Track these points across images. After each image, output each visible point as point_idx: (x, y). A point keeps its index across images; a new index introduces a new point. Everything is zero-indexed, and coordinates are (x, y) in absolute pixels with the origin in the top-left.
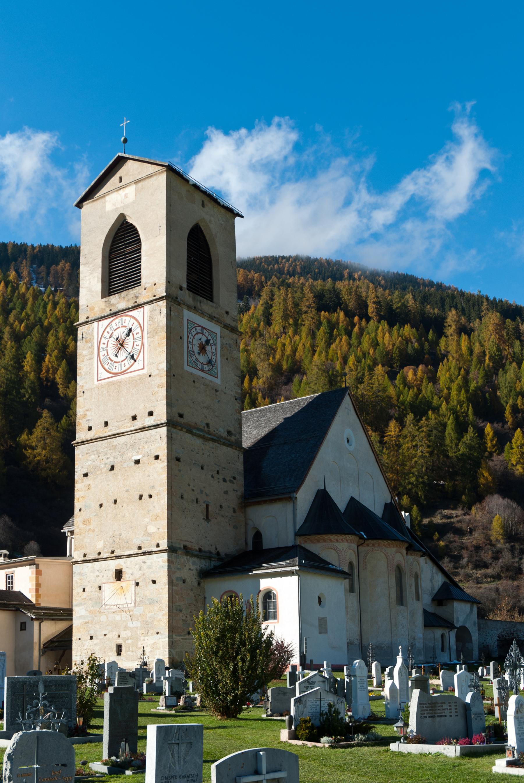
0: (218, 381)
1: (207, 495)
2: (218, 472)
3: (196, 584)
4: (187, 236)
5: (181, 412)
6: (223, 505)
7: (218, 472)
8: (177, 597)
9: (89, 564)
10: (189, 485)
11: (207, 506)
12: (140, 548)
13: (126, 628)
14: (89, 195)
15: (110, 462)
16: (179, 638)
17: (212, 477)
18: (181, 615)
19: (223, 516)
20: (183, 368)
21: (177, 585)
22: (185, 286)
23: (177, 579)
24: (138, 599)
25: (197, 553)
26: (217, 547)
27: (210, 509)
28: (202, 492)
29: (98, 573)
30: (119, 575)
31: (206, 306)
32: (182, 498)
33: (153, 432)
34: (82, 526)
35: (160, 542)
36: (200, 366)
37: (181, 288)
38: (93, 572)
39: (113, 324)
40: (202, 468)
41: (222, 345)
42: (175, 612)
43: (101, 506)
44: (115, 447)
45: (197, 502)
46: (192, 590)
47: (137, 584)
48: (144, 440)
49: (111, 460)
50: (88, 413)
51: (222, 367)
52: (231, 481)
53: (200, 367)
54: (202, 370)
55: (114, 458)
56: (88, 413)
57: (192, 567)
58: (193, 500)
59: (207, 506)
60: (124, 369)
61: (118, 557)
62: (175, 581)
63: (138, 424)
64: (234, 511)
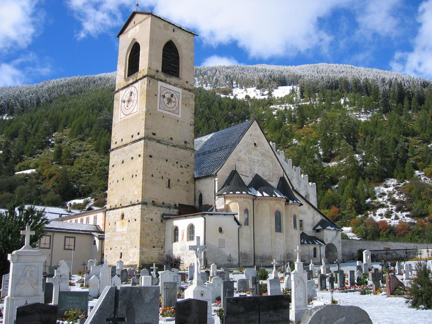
0: (180, 116)
1: (169, 174)
2: (177, 163)
3: (160, 221)
4: (163, 46)
5: (154, 132)
6: (180, 180)
7: (177, 163)
9: (112, 211)
10: (157, 169)
11: (169, 180)
13: (124, 244)
14: (122, 32)
15: (122, 159)
16: (147, 249)
17: (173, 165)
18: (149, 237)
19: (179, 185)
21: (147, 222)
22: (160, 70)
23: (147, 218)
24: (129, 229)
25: (162, 205)
26: (175, 201)
27: (171, 182)
28: (166, 173)
29: (114, 216)
30: (123, 216)
31: (174, 80)
32: (152, 176)
33: (139, 143)
34: (110, 192)
35: (139, 199)
37: (157, 71)
38: (113, 215)
39: (127, 91)
40: (167, 161)
42: (145, 235)
43: (118, 181)
44: (124, 151)
45: (162, 178)
46: (157, 224)
47: (129, 221)
48: (135, 147)
49: (123, 158)
50: (116, 135)
52: (185, 167)
53: (168, 109)
55: (124, 157)
56: (116, 135)
58: (160, 177)
59: (169, 180)
60: (130, 112)
61: (122, 207)
62: (145, 219)
63: (134, 139)
64: (187, 182)
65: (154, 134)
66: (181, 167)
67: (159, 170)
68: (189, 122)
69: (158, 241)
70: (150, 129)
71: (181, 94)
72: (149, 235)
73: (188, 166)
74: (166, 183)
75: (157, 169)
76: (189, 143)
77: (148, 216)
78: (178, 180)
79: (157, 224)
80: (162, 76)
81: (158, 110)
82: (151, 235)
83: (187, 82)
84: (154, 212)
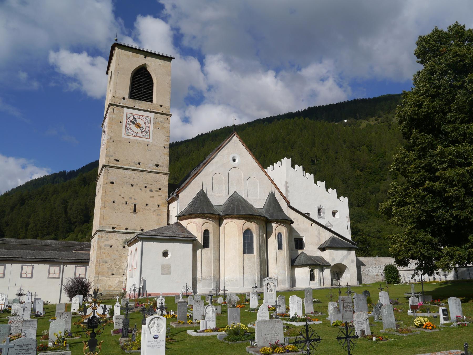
0: (150, 140)
1: (135, 199)
2: (146, 187)
6: (149, 204)
7: (146, 187)
8: (104, 255)
11: (135, 205)
12: (127, 229)
16: (104, 277)
18: (106, 265)
19: (148, 210)
20: (121, 137)
21: (104, 249)
22: (127, 96)
23: (105, 245)
25: (124, 231)
27: (137, 207)
31: (144, 105)
32: (114, 202)
37: (124, 98)
41: (154, 123)
45: (126, 204)
51: (153, 133)
52: (156, 191)
53: (136, 135)
57: (118, 239)
59: (135, 205)
62: (103, 247)
65: (117, 161)
66: (151, 191)
67: (122, 196)
68: (163, 145)
69: (119, 268)
70: (112, 156)
71: (152, 119)
72: (107, 263)
73: (160, 189)
74: (130, 209)
75: (120, 195)
76: (162, 167)
77: (106, 243)
78: (147, 205)
79: (117, 251)
80: (131, 103)
81: (123, 136)
82: (109, 263)
83: (161, 106)
84: (114, 238)
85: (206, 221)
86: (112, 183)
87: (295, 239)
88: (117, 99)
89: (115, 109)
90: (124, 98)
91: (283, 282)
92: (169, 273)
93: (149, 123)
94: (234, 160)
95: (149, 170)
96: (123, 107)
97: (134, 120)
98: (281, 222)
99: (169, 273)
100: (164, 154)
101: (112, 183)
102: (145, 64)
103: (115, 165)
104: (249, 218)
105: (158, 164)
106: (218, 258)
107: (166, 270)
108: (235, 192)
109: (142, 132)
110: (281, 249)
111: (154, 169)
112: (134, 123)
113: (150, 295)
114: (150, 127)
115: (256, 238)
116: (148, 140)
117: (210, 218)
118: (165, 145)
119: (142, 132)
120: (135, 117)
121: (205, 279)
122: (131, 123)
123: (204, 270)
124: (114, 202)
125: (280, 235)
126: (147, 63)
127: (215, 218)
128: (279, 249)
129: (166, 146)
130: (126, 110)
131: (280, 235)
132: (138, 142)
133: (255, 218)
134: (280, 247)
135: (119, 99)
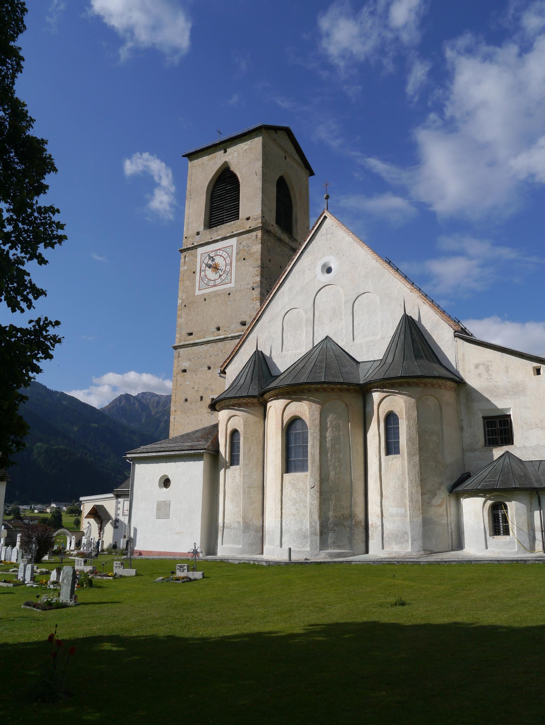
5: (189, 332)
20: (194, 296)
22: (201, 228)
32: (186, 400)
36: (212, 283)
54: (215, 286)
65: (191, 334)
80: (208, 235)
83: (248, 219)
85: (233, 412)
86: (185, 371)
87: (484, 418)
88: (190, 239)
89: (187, 255)
90: (198, 233)
91: (399, 538)
92: (167, 516)
93: (230, 256)
94: (329, 270)
95: (229, 336)
96: (196, 247)
97: (210, 262)
98: (392, 386)
99: (167, 516)
100: (253, 300)
101: (185, 371)
102: (226, 163)
103: (191, 342)
104: (295, 393)
105: (245, 320)
106: (260, 484)
107: (163, 510)
108: (327, 337)
109: (220, 276)
110: (397, 452)
111: (238, 331)
112: (210, 266)
113: (140, 554)
114: (231, 263)
115: (409, 427)
116: (229, 286)
117: (240, 405)
118: (254, 283)
119: (220, 276)
120: (211, 255)
121: (229, 527)
122: (207, 268)
123: (230, 510)
124: (186, 400)
125: (391, 419)
126: (226, 160)
127: (253, 404)
128: (388, 453)
129: (254, 286)
130: (200, 250)
131: (391, 419)
132: (216, 294)
133: (309, 390)
134: (391, 447)
135: (193, 237)
